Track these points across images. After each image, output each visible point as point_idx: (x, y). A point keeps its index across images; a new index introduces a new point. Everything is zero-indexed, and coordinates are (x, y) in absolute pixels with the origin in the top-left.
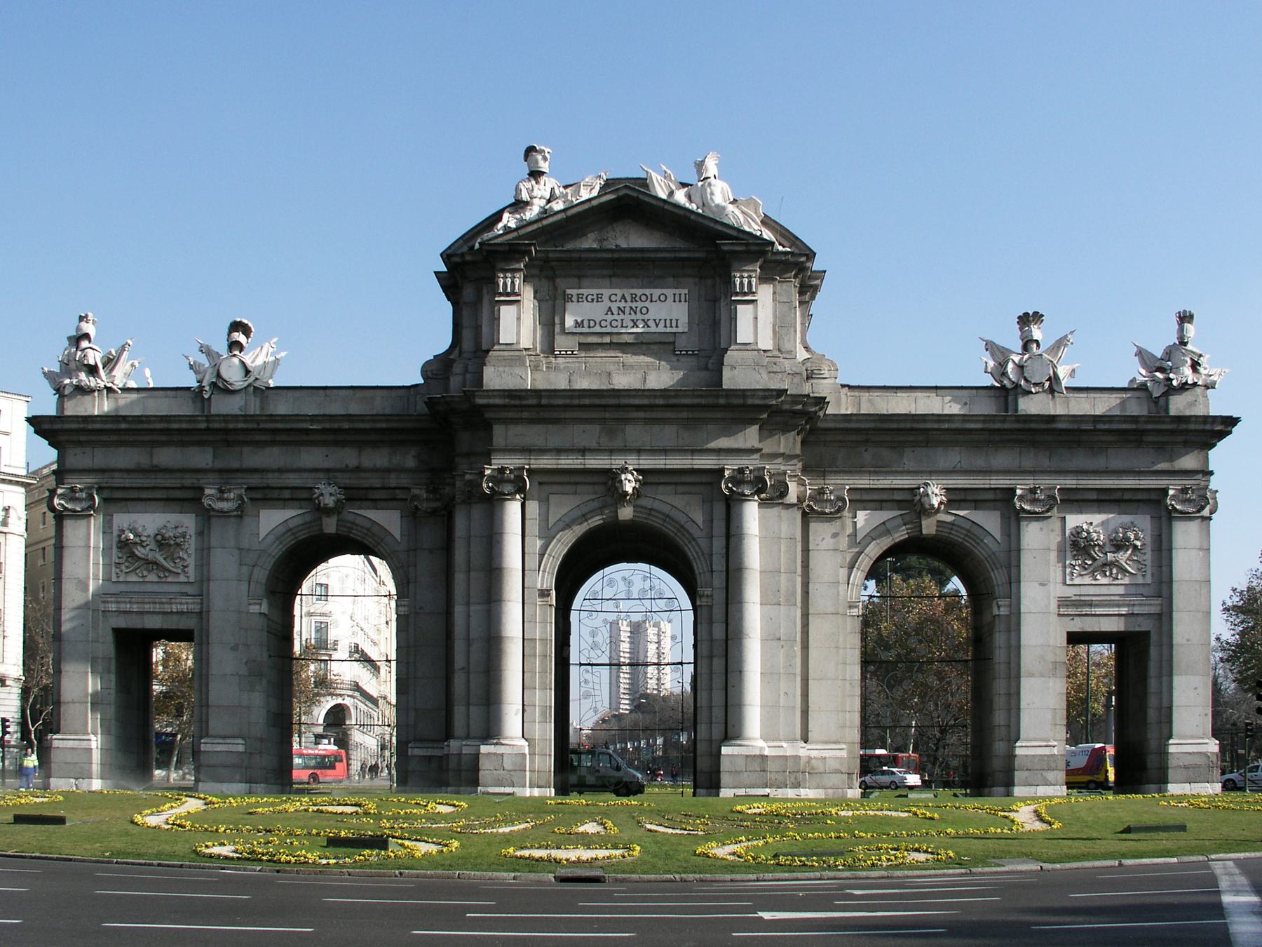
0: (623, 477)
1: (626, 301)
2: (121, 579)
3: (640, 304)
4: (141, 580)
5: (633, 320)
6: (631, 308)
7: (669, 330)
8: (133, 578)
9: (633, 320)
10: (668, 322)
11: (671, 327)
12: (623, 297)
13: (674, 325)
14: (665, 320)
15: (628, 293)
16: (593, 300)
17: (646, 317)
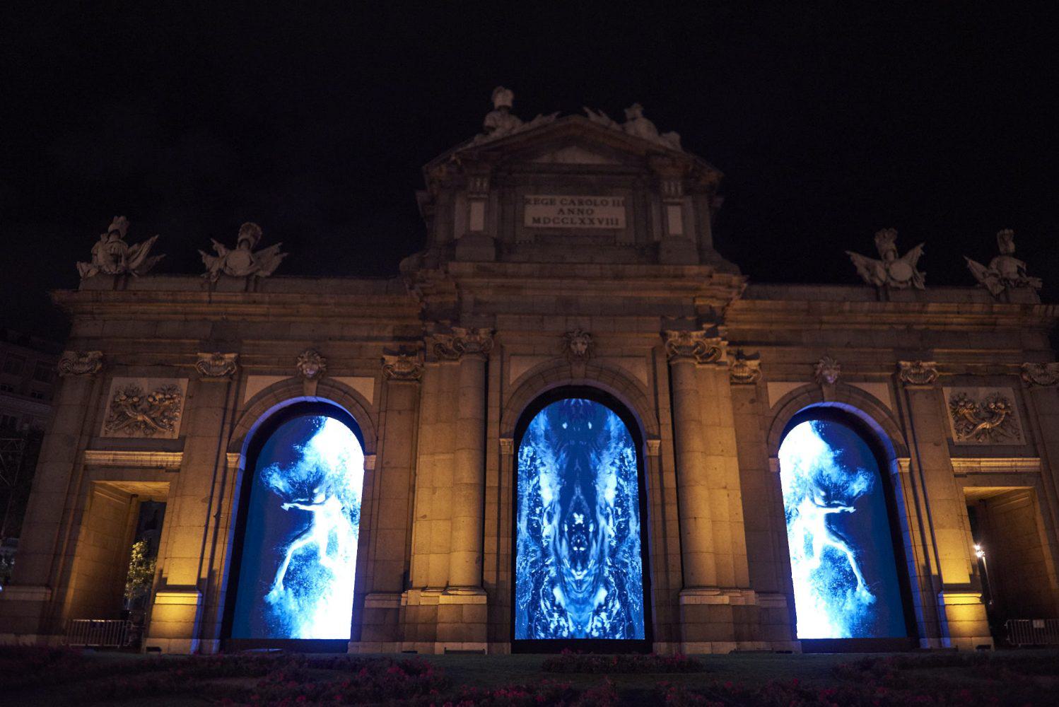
0: (579, 340)
1: (574, 204)
2: (109, 435)
3: (586, 207)
4: (127, 436)
5: (580, 219)
6: (579, 210)
7: (610, 226)
8: (120, 435)
9: (580, 219)
10: (610, 221)
11: (612, 224)
12: (573, 202)
13: (614, 222)
14: (607, 220)
15: (576, 199)
16: (547, 204)
17: (591, 217)
